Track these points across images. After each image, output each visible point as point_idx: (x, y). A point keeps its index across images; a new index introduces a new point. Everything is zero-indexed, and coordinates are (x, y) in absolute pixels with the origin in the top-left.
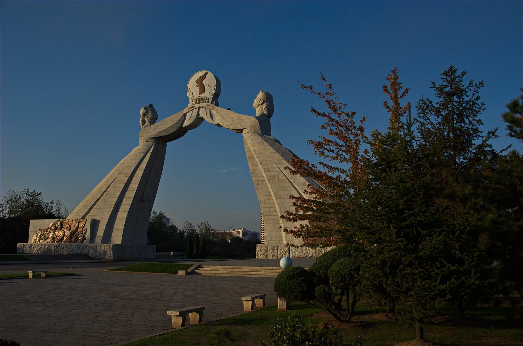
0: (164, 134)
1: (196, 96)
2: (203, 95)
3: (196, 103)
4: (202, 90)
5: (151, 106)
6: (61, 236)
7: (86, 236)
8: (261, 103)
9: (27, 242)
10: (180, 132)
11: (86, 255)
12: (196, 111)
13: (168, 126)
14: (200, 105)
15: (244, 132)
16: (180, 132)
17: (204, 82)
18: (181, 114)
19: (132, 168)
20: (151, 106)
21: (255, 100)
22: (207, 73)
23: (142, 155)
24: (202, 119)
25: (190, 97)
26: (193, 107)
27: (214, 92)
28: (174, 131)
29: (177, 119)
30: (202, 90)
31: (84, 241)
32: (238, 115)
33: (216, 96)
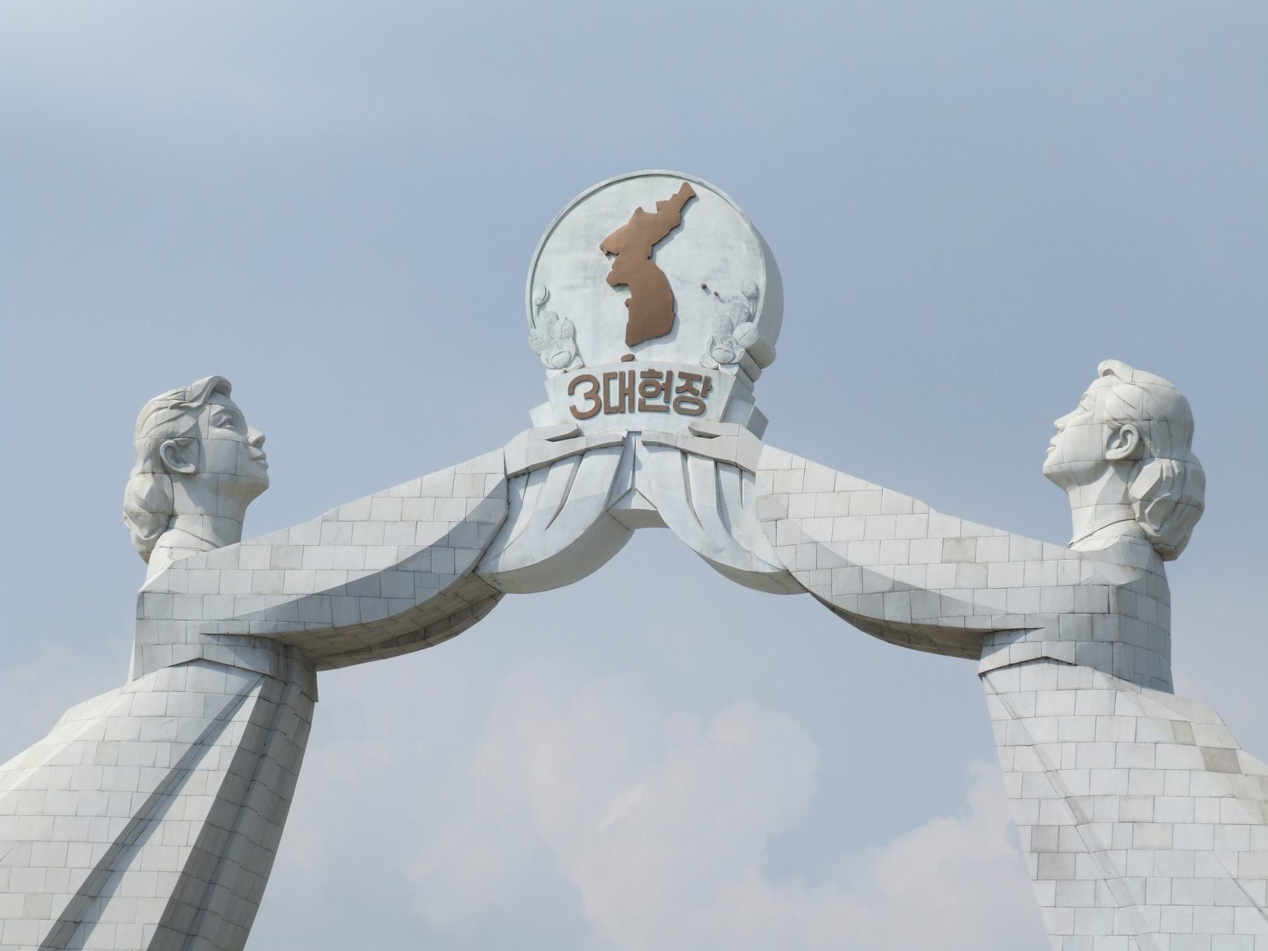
0: (347, 616)
2: (657, 356)
4: (653, 317)
5: (219, 389)
8: (1115, 453)
10: (439, 605)
12: (600, 469)
16: (439, 605)
17: (669, 258)
18: (488, 470)
19: (87, 859)
20: (219, 389)
21: (1070, 423)
22: (687, 198)
23: (167, 760)
24: (652, 519)
25: (552, 356)
26: (577, 434)
27: (745, 333)
28: (426, 594)
29: (456, 512)
30: (653, 317)
32: (950, 525)
33: (754, 362)
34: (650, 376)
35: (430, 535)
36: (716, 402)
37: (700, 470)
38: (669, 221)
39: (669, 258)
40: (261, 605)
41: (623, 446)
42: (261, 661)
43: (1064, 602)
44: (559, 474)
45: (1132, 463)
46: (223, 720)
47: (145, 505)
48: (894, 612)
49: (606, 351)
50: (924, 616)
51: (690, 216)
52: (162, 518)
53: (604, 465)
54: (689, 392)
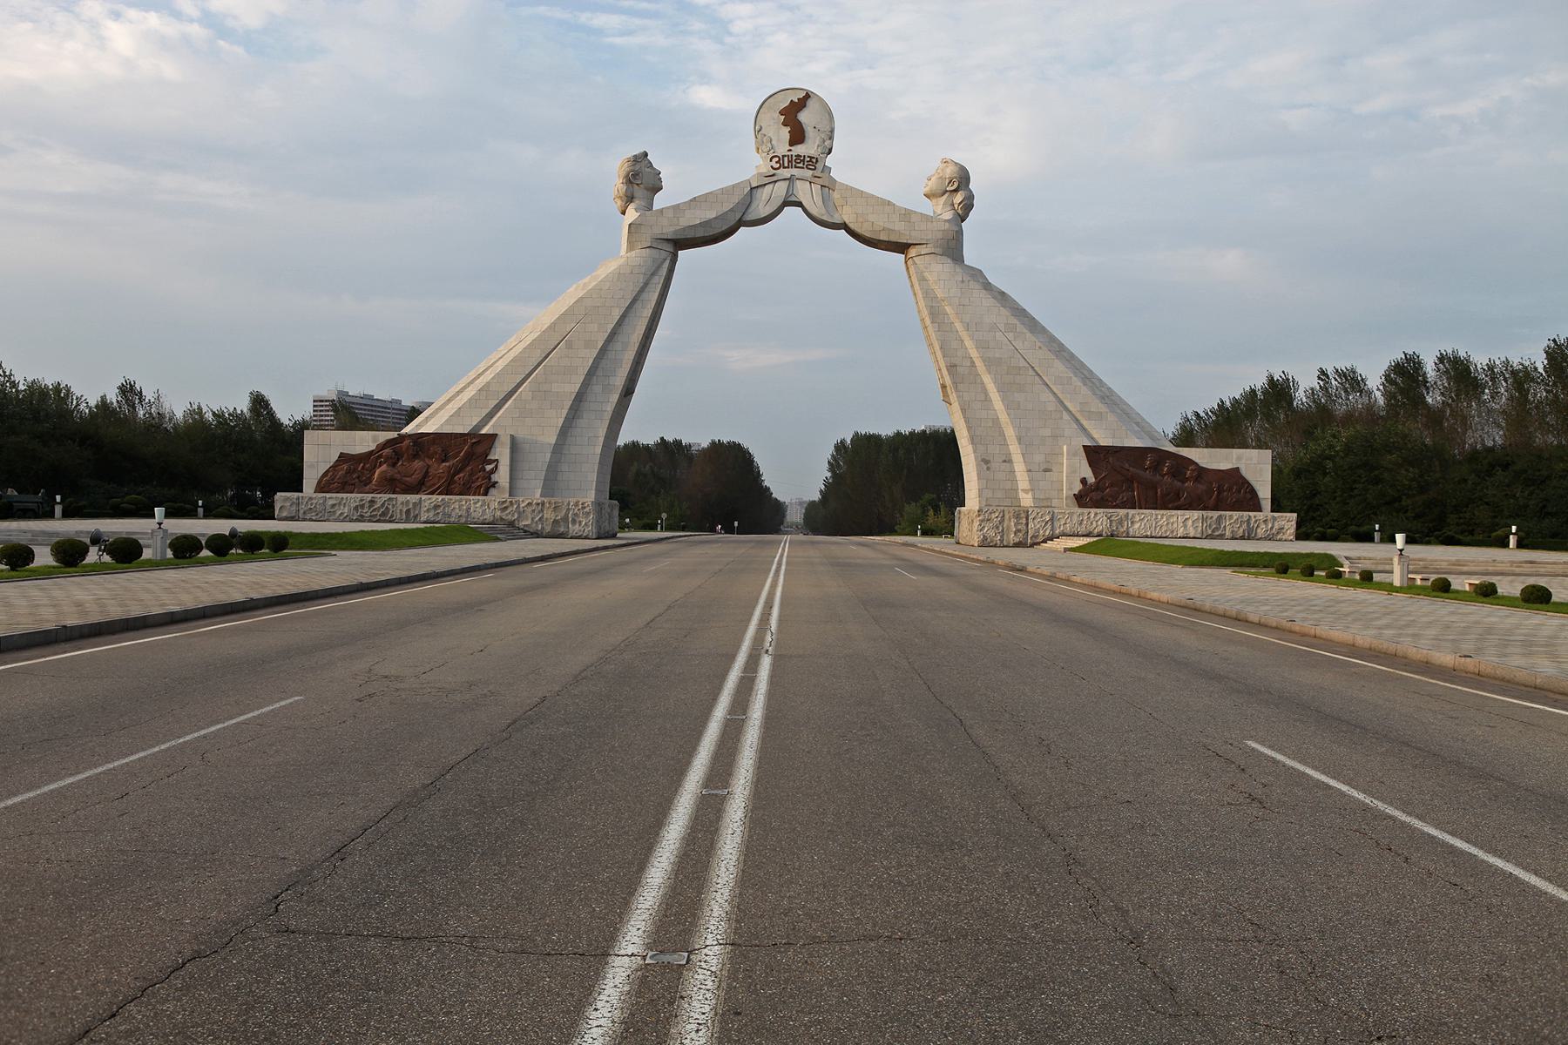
0: (700, 233)
1: (783, 148)
2: (800, 150)
3: (782, 166)
4: (798, 136)
5: (646, 154)
6: (416, 477)
7: (495, 477)
9: (301, 491)
11: (511, 524)
12: (781, 189)
13: (711, 215)
14: (794, 171)
15: (913, 252)
17: (804, 117)
19: (617, 314)
23: (642, 280)
24: (799, 204)
31: (492, 491)
34: (798, 156)
35: (727, 207)
36: (819, 166)
37: (816, 188)
39: (804, 117)
40: (672, 229)
41: (790, 179)
42: (670, 248)
43: (940, 235)
44: (768, 188)
45: (956, 191)
46: (659, 267)
47: (622, 192)
48: (883, 237)
49: (783, 148)
50: (894, 238)
51: (810, 103)
52: (630, 199)
53: (784, 185)
54: (812, 162)
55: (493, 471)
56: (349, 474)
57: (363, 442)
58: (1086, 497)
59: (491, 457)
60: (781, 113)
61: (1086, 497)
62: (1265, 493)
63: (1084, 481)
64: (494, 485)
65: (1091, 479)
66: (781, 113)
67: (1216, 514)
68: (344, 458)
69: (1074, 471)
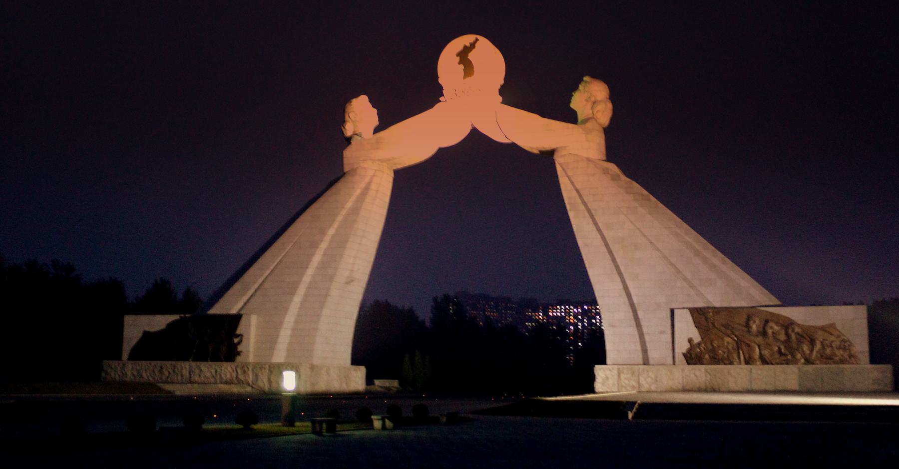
7: (240, 348)
9: (119, 358)
31: (239, 359)
38: (473, 46)
55: (239, 343)
56: (151, 347)
57: (159, 322)
58: (692, 358)
59: (238, 332)
60: (458, 55)
61: (692, 358)
62: (861, 346)
63: (690, 341)
64: (239, 353)
65: (697, 339)
66: (458, 55)
67: (810, 368)
68: (146, 334)
69: (687, 331)
